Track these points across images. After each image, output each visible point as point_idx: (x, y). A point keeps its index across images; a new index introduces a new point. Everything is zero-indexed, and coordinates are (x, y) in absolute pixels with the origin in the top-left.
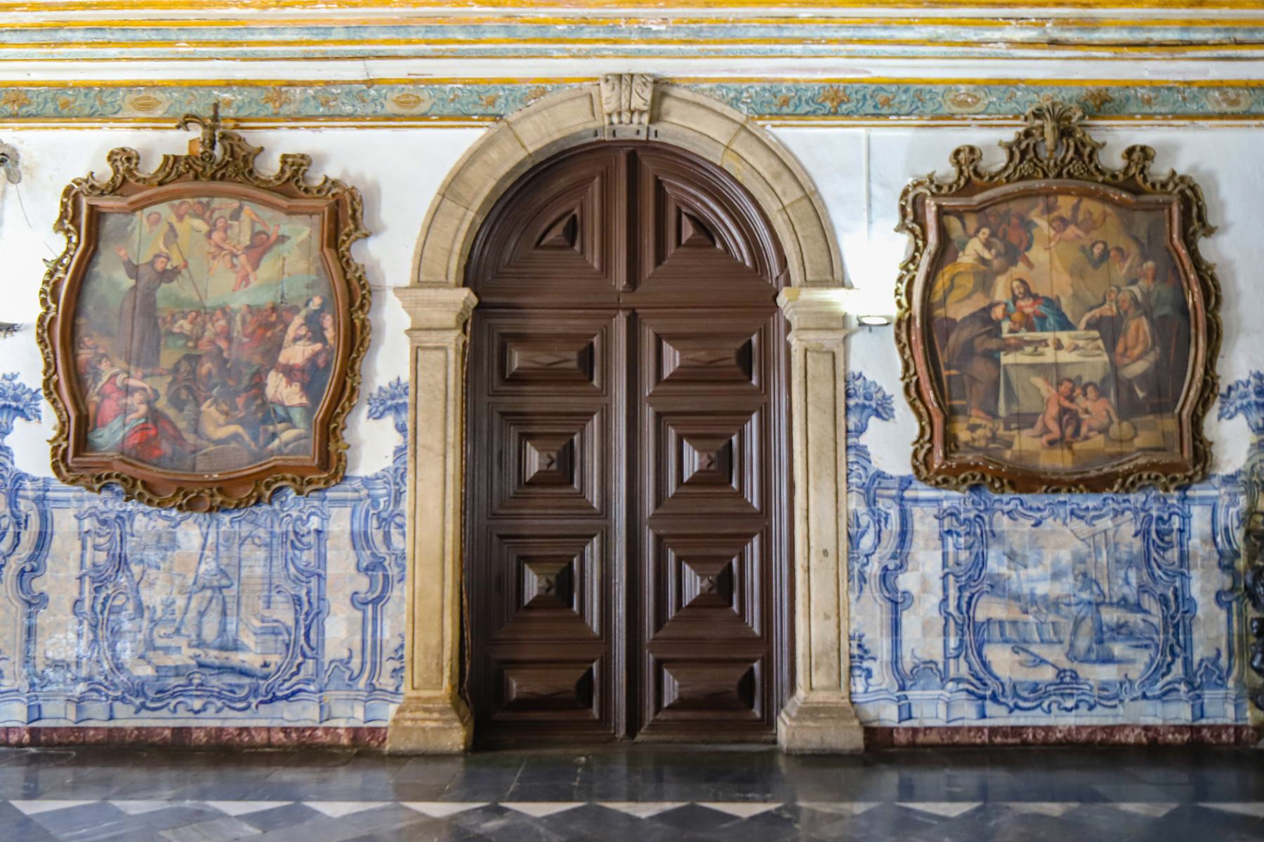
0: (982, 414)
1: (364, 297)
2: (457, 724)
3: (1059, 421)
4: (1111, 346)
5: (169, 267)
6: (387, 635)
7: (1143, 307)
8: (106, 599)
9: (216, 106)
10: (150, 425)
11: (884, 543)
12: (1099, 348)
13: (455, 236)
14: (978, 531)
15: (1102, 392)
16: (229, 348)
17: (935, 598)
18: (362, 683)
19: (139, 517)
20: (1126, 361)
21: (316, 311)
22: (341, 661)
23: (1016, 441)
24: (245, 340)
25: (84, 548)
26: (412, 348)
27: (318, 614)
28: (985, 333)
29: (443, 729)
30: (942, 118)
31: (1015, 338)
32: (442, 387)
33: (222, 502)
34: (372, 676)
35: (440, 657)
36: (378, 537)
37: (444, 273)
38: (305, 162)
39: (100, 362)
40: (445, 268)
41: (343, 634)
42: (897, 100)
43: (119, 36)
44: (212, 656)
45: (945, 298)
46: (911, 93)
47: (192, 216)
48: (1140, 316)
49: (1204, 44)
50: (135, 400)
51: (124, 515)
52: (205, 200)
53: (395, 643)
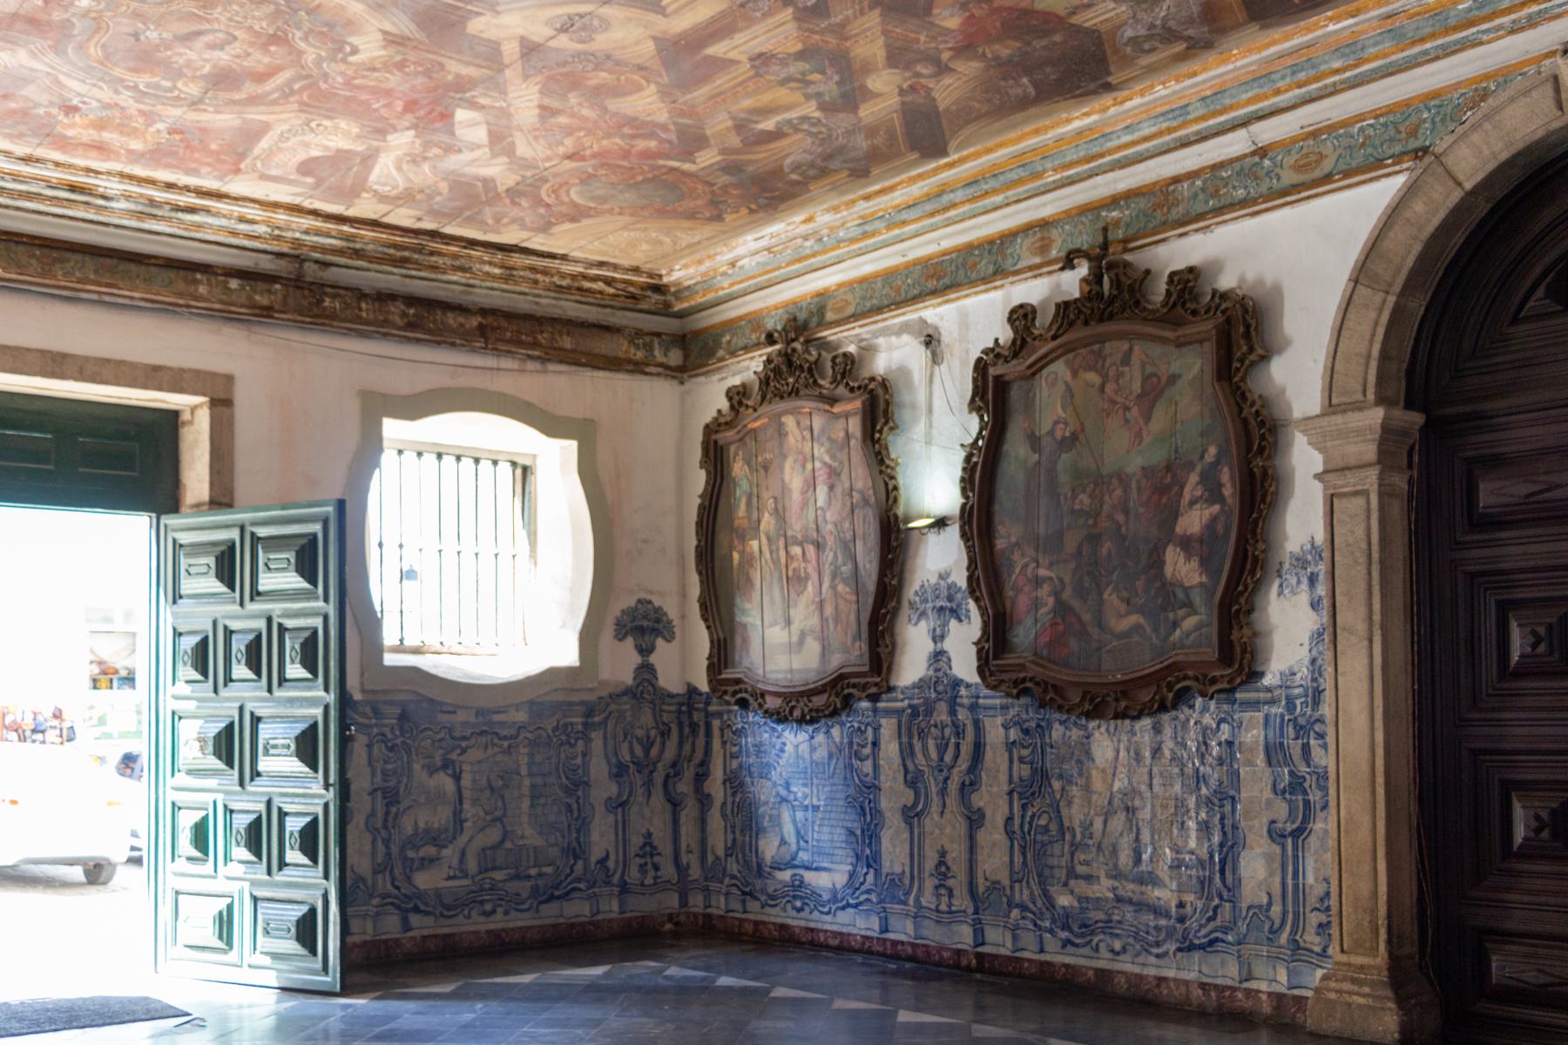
1: (1263, 437)
2: (1391, 1005)
5: (1067, 434)
6: (1310, 880)
8: (1032, 817)
9: (1105, 229)
10: (1059, 620)
13: (1373, 335)
16: (1127, 523)
18: (1284, 938)
19: (1056, 725)
21: (1211, 463)
22: (1260, 907)
24: (1141, 510)
25: (1011, 761)
26: (1325, 497)
27: (1232, 847)
29: (1370, 1007)
32: (1364, 546)
33: (1126, 707)
34: (1294, 931)
35: (1373, 911)
36: (1296, 752)
37: (1360, 388)
38: (1191, 277)
39: (1012, 552)
40: (1360, 380)
41: (1261, 873)
43: (992, 184)
44: (1128, 889)
47: (1085, 369)
50: (1044, 592)
51: (1043, 724)
52: (1096, 347)
53: (1319, 890)
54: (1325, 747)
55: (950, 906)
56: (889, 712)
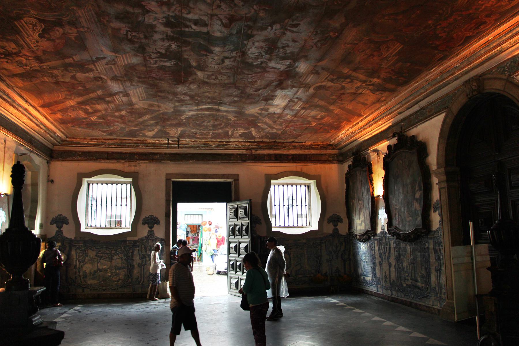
22: (434, 288)
34: (440, 294)
54: (442, 249)
55: (387, 285)
56: (377, 240)
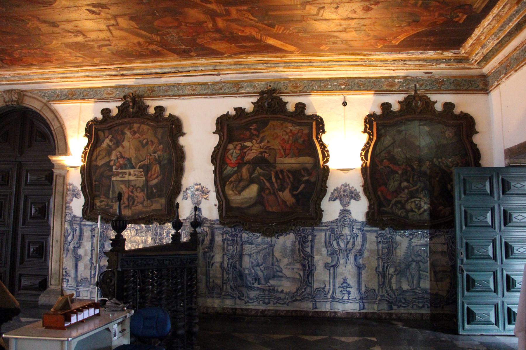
0: (104, 197)
3: (128, 200)
4: (146, 175)
7: (158, 161)
11: (75, 239)
12: (142, 175)
14: (103, 236)
15: (142, 191)
17: (88, 258)
20: (151, 179)
23: (114, 206)
28: (108, 170)
30: (101, 100)
31: (117, 172)
42: (90, 93)
45: (96, 158)
46: (94, 91)
48: (156, 164)
49: (170, 73)
